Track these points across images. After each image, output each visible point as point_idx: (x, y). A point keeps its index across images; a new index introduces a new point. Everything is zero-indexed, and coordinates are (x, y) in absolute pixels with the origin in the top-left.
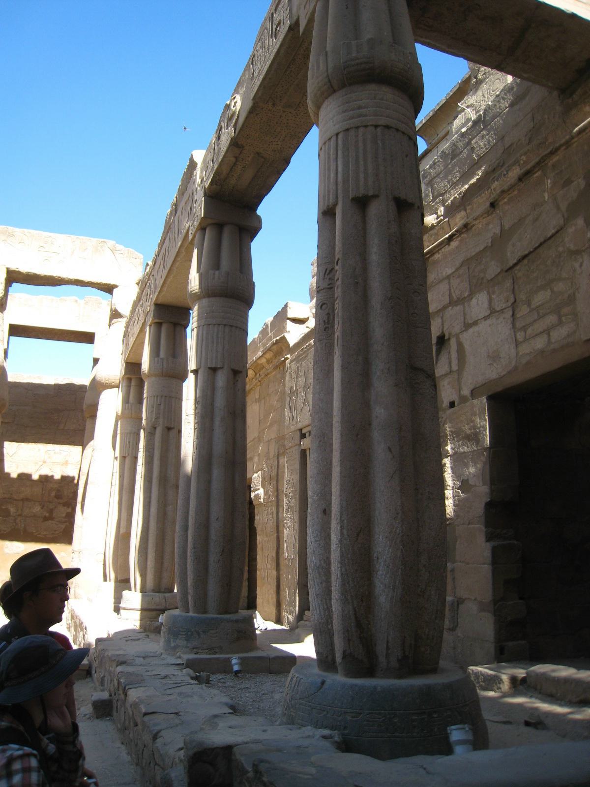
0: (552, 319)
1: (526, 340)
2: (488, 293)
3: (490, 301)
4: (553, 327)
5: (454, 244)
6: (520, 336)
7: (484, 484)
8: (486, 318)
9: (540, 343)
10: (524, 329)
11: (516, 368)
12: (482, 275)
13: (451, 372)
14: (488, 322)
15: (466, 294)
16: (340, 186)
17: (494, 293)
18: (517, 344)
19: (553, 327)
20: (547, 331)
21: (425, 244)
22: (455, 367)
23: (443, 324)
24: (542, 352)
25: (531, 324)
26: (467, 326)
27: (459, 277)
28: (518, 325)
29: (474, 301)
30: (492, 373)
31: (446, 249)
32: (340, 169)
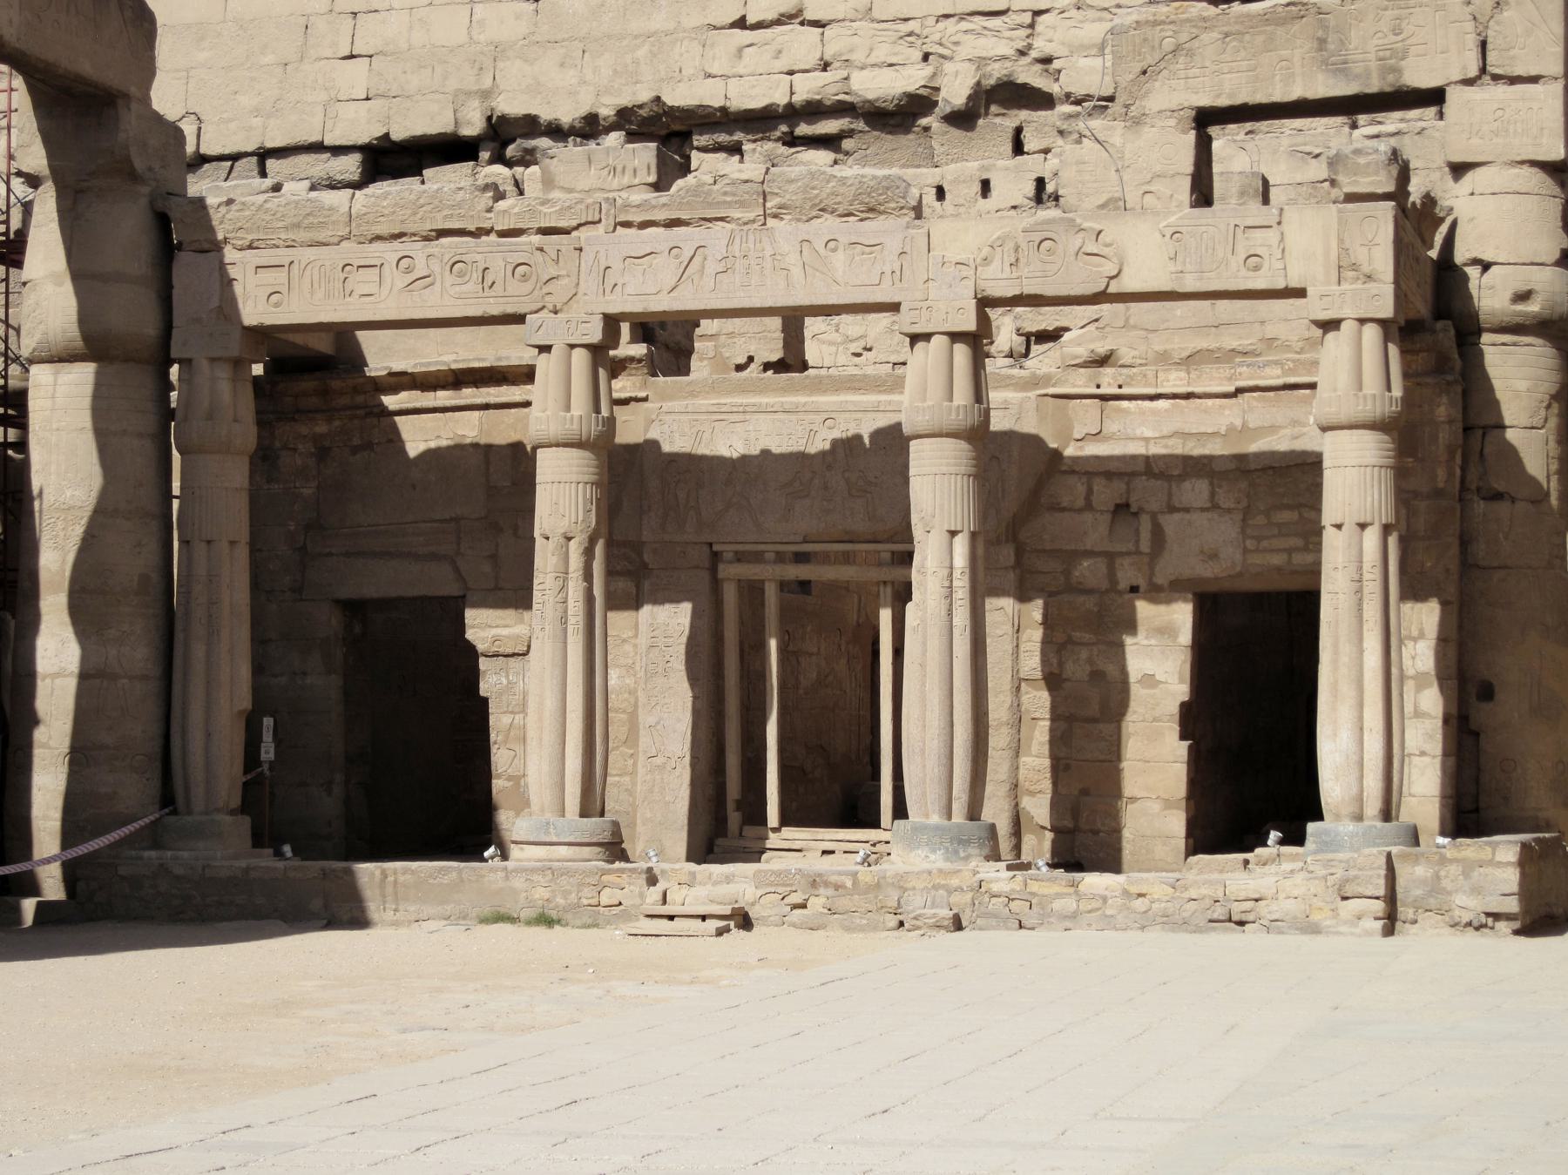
0: (1299, 542)
1: (1257, 550)
2: (1211, 484)
3: (1213, 494)
4: (1297, 549)
5: (1162, 403)
6: (1250, 544)
7: (1181, 681)
8: (1203, 510)
9: (1277, 560)
10: (1259, 539)
11: (1240, 575)
13: (1138, 553)
14: (1205, 514)
15: (1176, 473)
17: (1220, 487)
18: (1246, 551)
19: (1297, 549)
20: (1290, 551)
22: (1145, 546)
23: (1128, 492)
24: (1279, 569)
25: (1267, 538)
26: (1172, 509)
28: (1249, 531)
29: (1187, 485)
30: (1206, 571)
31: (1147, 404)
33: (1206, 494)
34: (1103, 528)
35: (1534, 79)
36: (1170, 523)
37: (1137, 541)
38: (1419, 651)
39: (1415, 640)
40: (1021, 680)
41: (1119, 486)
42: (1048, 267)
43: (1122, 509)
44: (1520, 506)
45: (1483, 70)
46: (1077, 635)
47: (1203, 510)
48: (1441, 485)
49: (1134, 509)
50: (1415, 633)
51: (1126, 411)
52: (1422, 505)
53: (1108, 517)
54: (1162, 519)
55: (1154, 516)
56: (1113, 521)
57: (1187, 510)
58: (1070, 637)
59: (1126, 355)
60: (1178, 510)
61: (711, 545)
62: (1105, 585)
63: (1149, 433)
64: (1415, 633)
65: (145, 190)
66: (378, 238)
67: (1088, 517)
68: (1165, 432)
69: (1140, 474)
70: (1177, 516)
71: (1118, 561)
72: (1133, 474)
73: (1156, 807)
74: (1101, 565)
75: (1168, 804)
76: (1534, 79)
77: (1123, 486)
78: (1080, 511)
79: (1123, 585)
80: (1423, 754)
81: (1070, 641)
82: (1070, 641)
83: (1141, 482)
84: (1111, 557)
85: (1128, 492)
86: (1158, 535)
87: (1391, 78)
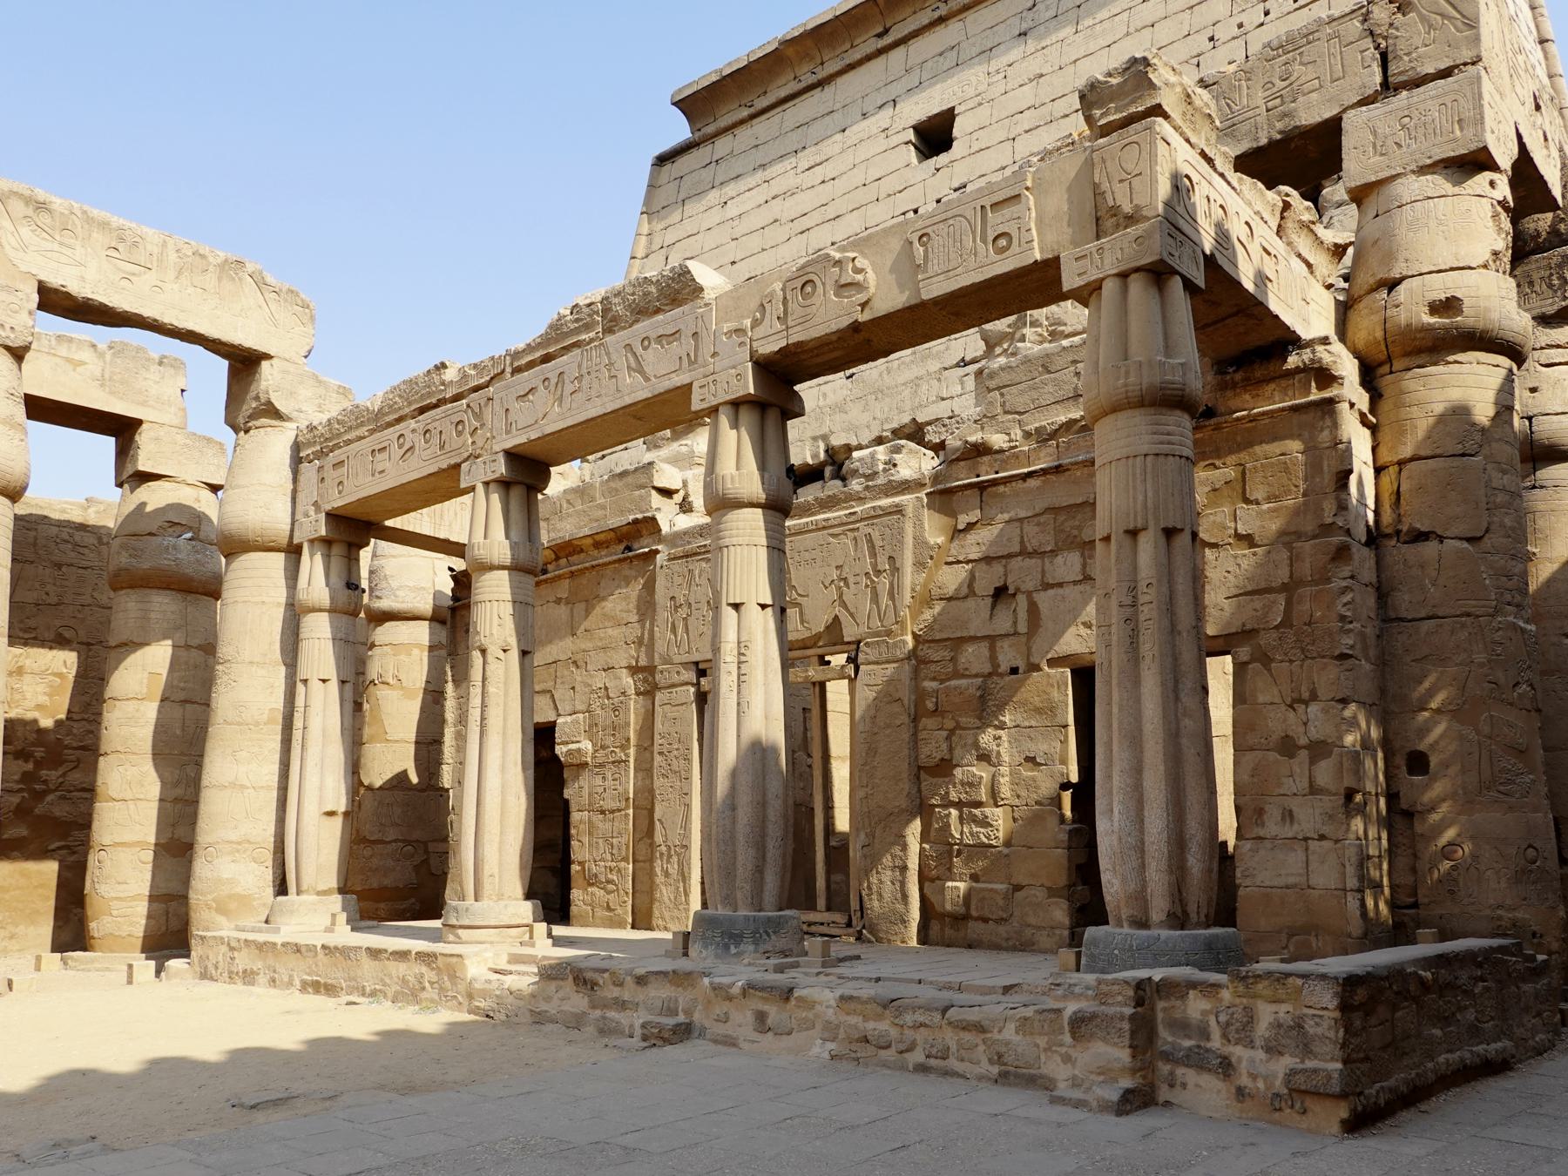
2: (1082, 555)
3: (1084, 566)
5: (1033, 483)
8: (1075, 583)
12: (1075, 532)
13: (1016, 633)
14: (1080, 587)
16: (1150, 512)
21: (983, 468)
22: (1022, 628)
23: (1006, 575)
26: (1046, 586)
27: (1038, 524)
29: (1059, 560)
31: (1020, 485)
32: (1150, 494)
33: (1078, 567)
34: (986, 613)
35: (1445, 73)
36: (1044, 600)
37: (1015, 623)
38: (1311, 716)
39: (1306, 703)
40: (920, 768)
41: (998, 568)
42: (808, 310)
43: (1000, 593)
44: (1450, 544)
45: (1385, 84)
46: (963, 720)
47: (1075, 583)
48: (1329, 520)
49: (1011, 591)
50: (1306, 695)
51: (1003, 495)
52: (1307, 546)
53: (989, 601)
54: (1038, 597)
55: (1029, 594)
56: (993, 607)
57: (1060, 585)
58: (958, 723)
59: (998, 440)
60: (1052, 586)
61: (697, 663)
62: (987, 668)
63: (1022, 514)
64: (1306, 695)
65: (293, 425)
66: (389, 425)
67: (971, 603)
68: (1037, 511)
69: (1016, 555)
70: (1051, 592)
71: (999, 644)
72: (1010, 556)
73: (1040, 894)
74: (983, 649)
75: (1052, 892)
76: (1445, 73)
77: (1001, 570)
78: (966, 597)
79: (1004, 667)
80: (1322, 837)
81: (958, 726)
82: (958, 726)
83: (1016, 563)
84: (992, 639)
85: (1006, 575)
86: (1033, 610)
87: (1279, 125)
